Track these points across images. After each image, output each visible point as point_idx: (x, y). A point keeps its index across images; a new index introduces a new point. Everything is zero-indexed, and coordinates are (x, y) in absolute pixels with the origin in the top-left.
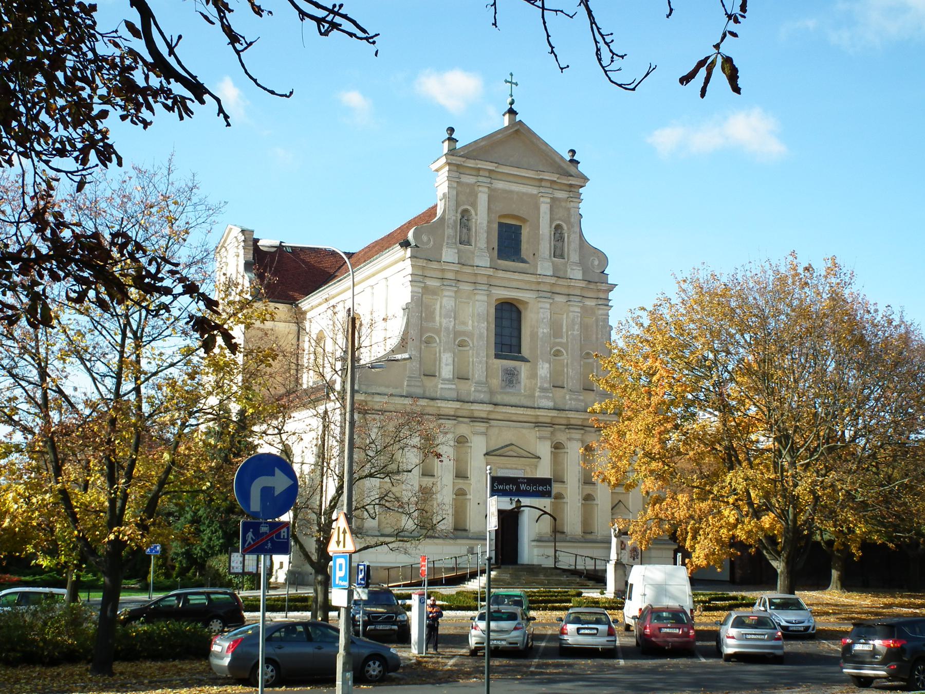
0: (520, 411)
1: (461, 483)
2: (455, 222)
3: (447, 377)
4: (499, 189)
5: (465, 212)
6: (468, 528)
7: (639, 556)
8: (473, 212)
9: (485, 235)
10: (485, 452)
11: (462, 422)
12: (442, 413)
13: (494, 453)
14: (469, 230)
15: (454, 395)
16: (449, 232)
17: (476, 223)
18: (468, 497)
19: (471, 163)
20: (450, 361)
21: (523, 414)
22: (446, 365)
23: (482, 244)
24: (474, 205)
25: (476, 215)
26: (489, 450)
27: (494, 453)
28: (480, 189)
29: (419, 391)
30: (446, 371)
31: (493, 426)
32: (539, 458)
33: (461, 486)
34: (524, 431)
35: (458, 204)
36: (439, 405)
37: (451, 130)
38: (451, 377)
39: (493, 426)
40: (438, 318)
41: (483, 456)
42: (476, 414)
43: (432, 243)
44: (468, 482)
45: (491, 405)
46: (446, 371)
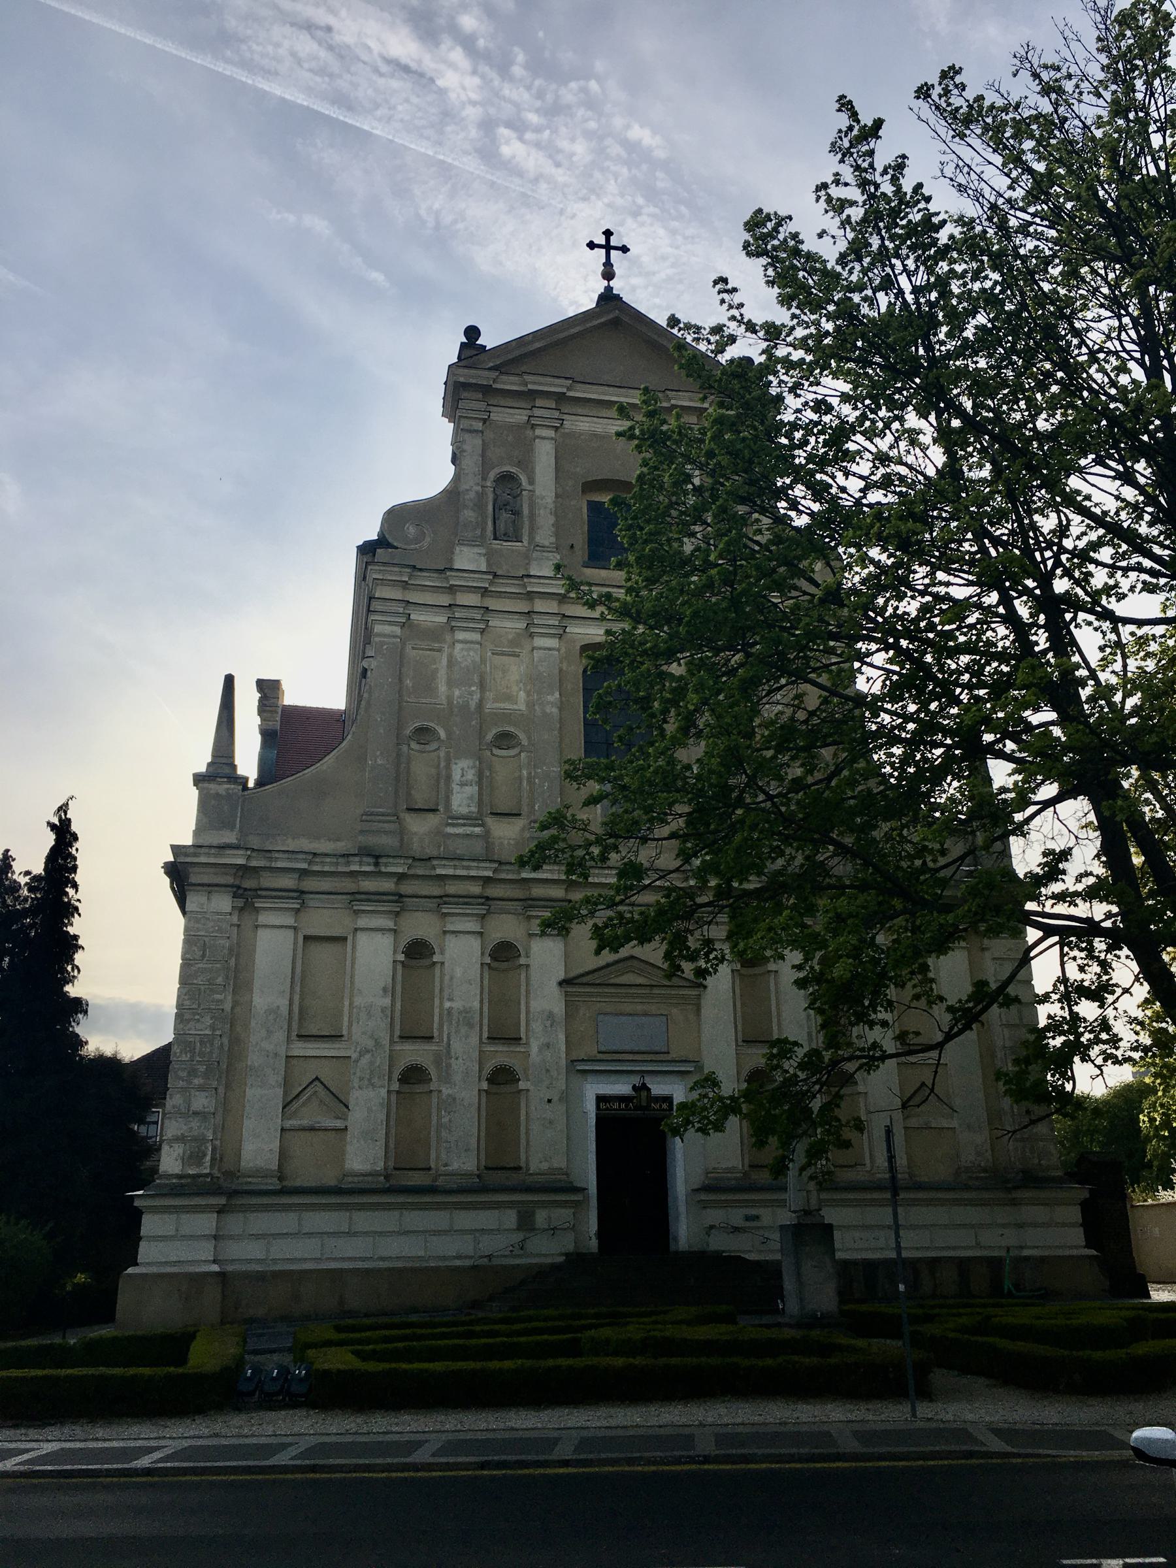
1: (501, 1055)
2: (481, 496)
3: (464, 810)
4: (581, 434)
5: (507, 479)
6: (523, 1164)
8: (523, 479)
9: (552, 520)
13: (585, 980)
14: (517, 513)
15: (478, 848)
16: (469, 515)
17: (531, 498)
18: (522, 1085)
19: (510, 383)
20: (471, 775)
22: (463, 784)
23: (545, 536)
24: (526, 463)
25: (531, 481)
26: (572, 974)
27: (585, 980)
28: (538, 432)
29: (386, 841)
30: (462, 800)
35: (486, 464)
37: (472, 332)
38: (474, 809)
40: (443, 688)
43: (428, 539)
46: (462, 800)
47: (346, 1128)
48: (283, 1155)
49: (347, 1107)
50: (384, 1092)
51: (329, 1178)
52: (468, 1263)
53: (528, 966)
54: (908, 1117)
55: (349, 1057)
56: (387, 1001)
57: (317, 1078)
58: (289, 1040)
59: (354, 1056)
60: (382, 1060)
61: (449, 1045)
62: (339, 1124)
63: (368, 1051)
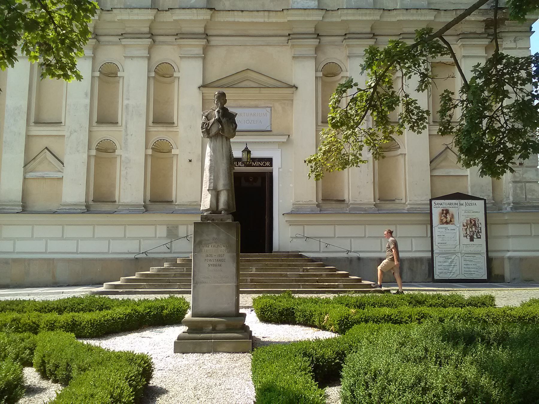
0: (260, 18)
6: (174, 199)
7: (483, 235)
10: (200, 83)
11: (164, 43)
12: (129, 30)
13: (215, 84)
21: (264, 23)
31: (216, 46)
32: (297, 88)
33: (162, 136)
34: (270, 50)
36: (119, 17)
39: (216, 46)
41: (197, 90)
42: (186, 29)
44: (174, 129)
45: (204, 11)
47: (62, 178)
48: (25, 193)
49: (63, 164)
50: (85, 156)
51: (54, 206)
52: (132, 256)
53: (179, 78)
54: (434, 169)
55: (64, 136)
56: (88, 101)
57: (46, 148)
58: (28, 124)
59: (66, 134)
60: (84, 137)
61: (126, 127)
62: (59, 175)
63: (75, 131)
